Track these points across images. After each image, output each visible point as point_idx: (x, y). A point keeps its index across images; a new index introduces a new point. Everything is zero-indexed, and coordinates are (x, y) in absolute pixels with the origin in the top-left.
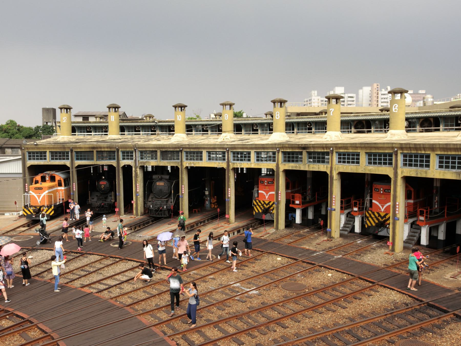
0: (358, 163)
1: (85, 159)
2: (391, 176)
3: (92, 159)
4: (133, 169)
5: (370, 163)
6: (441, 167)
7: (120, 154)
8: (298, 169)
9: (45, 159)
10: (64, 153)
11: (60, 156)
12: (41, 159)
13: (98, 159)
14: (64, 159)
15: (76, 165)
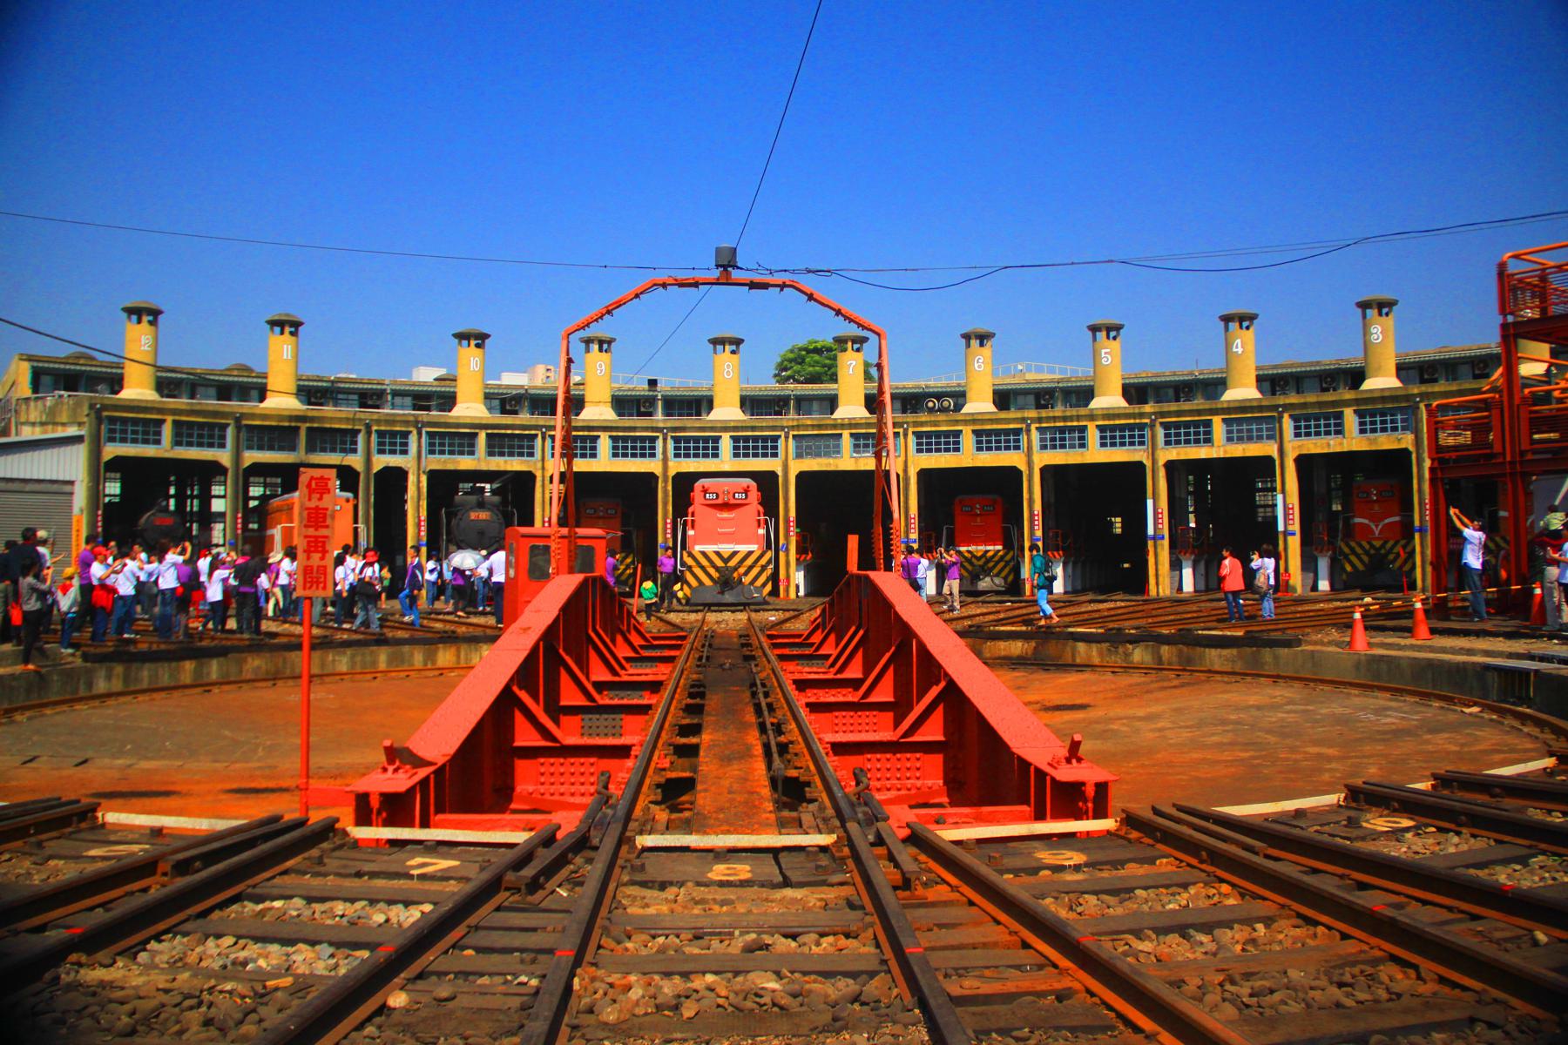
0: (957, 450)
1: (271, 448)
2: (1023, 467)
3: (293, 448)
4: (412, 479)
5: (979, 449)
6: (1103, 445)
7: (374, 437)
8: (832, 468)
9: (158, 442)
10: (211, 426)
11: (200, 436)
12: (146, 442)
13: (311, 448)
14: (211, 445)
15: (247, 464)
